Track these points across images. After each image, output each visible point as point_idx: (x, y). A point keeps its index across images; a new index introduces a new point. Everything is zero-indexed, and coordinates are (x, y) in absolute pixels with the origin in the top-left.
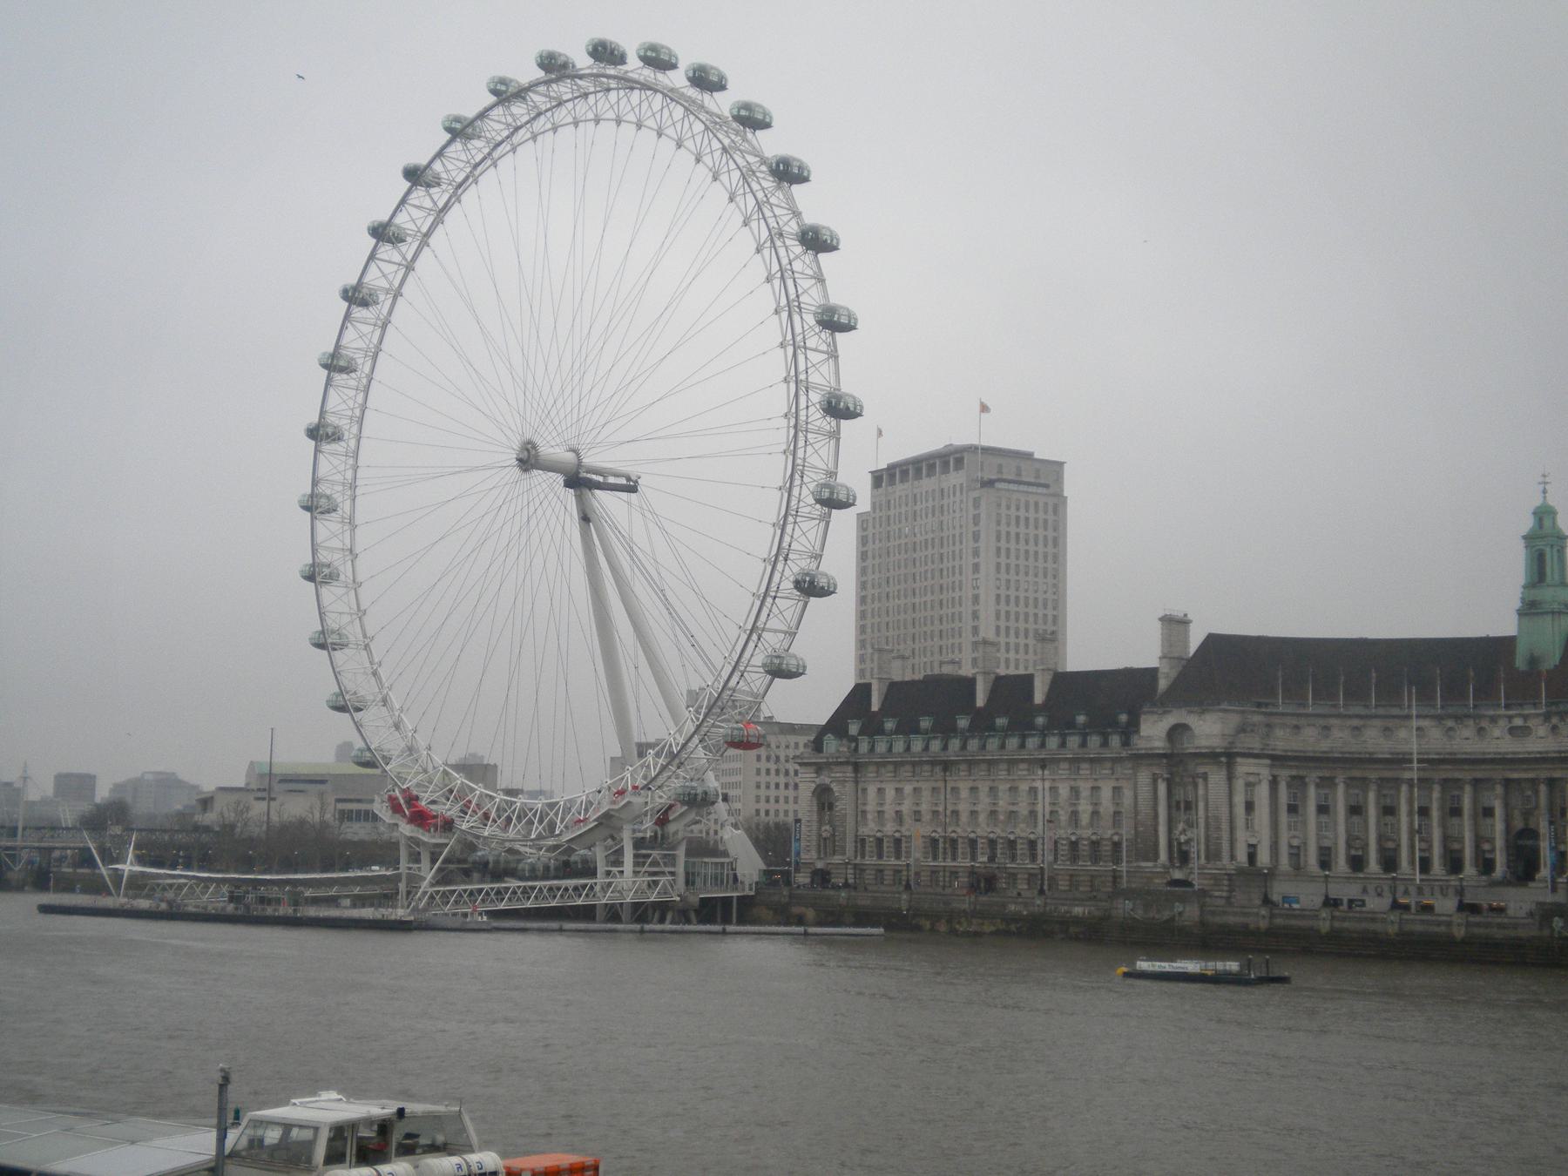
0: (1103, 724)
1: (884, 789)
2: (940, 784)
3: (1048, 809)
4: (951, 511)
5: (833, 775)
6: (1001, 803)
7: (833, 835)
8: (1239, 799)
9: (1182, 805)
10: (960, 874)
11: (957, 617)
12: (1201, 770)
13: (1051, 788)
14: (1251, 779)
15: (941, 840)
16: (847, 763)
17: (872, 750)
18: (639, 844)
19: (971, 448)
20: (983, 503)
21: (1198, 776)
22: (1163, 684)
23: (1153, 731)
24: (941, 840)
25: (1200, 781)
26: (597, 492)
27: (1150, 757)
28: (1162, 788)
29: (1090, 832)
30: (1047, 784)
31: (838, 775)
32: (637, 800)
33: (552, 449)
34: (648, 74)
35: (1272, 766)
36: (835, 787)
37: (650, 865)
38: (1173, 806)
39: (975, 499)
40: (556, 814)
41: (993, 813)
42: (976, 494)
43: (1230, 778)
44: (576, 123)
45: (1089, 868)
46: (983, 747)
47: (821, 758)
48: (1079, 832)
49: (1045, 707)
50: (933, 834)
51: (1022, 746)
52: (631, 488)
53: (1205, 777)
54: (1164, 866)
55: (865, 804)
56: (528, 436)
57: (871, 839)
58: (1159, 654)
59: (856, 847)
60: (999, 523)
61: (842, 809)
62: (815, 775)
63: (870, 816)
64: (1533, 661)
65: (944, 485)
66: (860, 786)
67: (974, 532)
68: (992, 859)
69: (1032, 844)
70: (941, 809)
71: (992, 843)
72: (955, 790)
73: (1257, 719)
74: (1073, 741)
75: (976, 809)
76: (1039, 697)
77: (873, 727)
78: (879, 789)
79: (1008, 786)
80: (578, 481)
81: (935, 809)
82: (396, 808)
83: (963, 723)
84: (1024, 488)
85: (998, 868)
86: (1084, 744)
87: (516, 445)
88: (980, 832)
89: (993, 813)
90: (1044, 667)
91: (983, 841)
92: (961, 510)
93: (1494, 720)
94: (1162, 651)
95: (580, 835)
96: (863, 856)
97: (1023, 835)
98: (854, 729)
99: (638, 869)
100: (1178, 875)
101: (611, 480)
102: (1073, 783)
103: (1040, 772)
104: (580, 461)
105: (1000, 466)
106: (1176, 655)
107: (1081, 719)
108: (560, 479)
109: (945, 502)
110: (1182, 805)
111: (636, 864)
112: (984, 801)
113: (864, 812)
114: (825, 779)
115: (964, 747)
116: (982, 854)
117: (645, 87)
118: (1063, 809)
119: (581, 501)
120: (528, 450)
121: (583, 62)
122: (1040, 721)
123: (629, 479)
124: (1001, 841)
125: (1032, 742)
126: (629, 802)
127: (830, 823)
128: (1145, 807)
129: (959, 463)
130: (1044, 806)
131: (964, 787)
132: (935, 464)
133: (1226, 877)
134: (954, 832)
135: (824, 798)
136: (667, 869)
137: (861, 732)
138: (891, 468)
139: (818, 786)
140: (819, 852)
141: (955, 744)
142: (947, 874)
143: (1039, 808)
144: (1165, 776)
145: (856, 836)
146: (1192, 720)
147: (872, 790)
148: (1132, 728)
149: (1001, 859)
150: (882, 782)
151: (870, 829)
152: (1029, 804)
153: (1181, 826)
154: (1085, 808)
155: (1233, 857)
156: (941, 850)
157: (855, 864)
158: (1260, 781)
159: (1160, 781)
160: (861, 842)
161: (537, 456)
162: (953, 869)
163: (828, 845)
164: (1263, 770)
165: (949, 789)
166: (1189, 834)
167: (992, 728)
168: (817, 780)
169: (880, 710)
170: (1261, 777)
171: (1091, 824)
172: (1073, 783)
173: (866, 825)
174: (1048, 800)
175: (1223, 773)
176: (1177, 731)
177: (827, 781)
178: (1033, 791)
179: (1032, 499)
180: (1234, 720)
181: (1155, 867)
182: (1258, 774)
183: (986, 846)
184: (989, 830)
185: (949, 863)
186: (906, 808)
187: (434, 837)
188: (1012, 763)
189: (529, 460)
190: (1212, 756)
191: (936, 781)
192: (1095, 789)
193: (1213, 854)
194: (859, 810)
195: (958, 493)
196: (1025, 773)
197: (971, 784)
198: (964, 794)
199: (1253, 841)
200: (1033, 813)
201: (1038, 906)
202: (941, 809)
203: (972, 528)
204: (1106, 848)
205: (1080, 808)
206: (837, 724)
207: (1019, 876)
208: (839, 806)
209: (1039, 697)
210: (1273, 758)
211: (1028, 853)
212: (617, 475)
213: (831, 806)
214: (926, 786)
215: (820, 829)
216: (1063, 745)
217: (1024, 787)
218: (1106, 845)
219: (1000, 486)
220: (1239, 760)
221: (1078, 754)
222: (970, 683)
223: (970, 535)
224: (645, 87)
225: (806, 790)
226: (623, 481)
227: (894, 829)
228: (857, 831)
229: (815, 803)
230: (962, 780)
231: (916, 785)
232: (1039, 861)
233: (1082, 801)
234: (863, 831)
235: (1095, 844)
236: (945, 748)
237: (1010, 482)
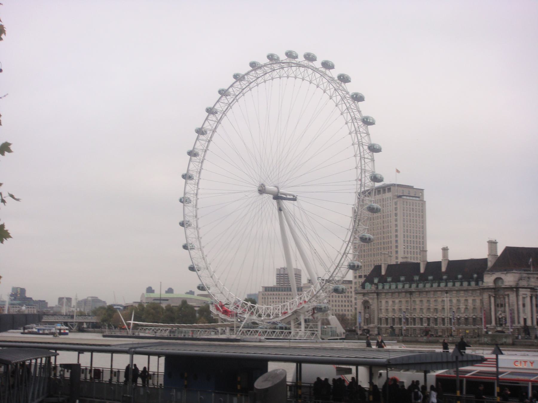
0: (468, 278)
1: (388, 301)
2: (409, 299)
4: (387, 206)
5: (369, 297)
6: (431, 305)
7: (370, 317)
8: (521, 303)
9: (499, 305)
10: (417, 330)
11: (390, 242)
12: (507, 293)
13: (450, 300)
14: (524, 296)
15: (410, 319)
16: (375, 293)
17: (383, 288)
18: (306, 321)
19: (393, 185)
20: (398, 203)
21: (505, 295)
22: (490, 264)
23: (489, 280)
24: (410, 319)
25: (506, 297)
26: (284, 201)
27: (488, 289)
28: (492, 299)
29: (464, 315)
30: (448, 299)
31: (371, 297)
32: (306, 306)
33: (270, 187)
34: (306, 63)
35: (530, 291)
36: (370, 301)
37: (310, 328)
38: (497, 306)
39: (395, 202)
40: (254, 310)
41: (429, 309)
42: (395, 200)
43: (517, 295)
44: (280, 77)
45: (464, 327)
46: (425, 286)
47: (365, 291)
48: (461, 315)
49: (446, 273)
51: (439, 286)
52: (294, 199)
53: (508, 295)
54: (494, 326)
55: (381, 307)
56: (262, 182)
57: (384, 318)
58: (488, 254)
59: (378, 321)
60: (404, 210)
62: (362, 297)
63: (383, 311)
65: (384, 197)
66: (379, 300)
67: (395, 213)
68: (428, 325)
69: (443, 319)
70: (409, 308)
71: (428, 319)
72: (414, 301)
73: (525, 275)
74: (458, 284)
75: (422, 307)
76: (444, 269)
77: (383, 280)
78: (386, 301)
80: (278, 197)
81: (407, 308)
82: (218, 309)
83: (416, 278)
84: (411, 198)
85: (431, 328)
86: (462, 285)
87: (258, 185)
88: (424, 315)
89: (429, 309)
90: (445, 259)
91: (425, 318)
92: (390, 206)
94: (489, 253)
95: (286, 318)
96: (381, 324)
97: (440, 316)
98: (376, 281)
99: (306, 329)
100: (499, 329)
101: (288, 197)
102: (458, 298)
103: (446, 295)
104: (279, 191)
105: (403, 191)
106: (494, 254)
107: (460, 276)
108: (272, 196)
109: (384, 203)
110: (499, 305)
111: (306, 328)
112: (425, 305)
113: (381, 309)
114: (366, 298)
115: (417, 286)
116: (425, 323)
117: (304, 66)
119: (279, 204)
120: (262, 187)
121: (301, 59)
122: (445, 277)
123: (294, 196)
124: (432, 318)
125: (443, 285)
126: (303, 307)
127: (368, 313)
128: (486, 305)
129: (389, 190)
130: (447, 305)
131: (418, 300)
132: (380, 190)
133: (517, 330)
134: (414, 316)
135: (366, 305)
136: (315, 329)
137: (379, 282)
139: (364, 301)
140: (364, 323)
141: (414, 286)
142: (412, 330)
143: (446, 307)
144: (494, 295)
145: (378, 317)
146: (503, 276)
147: (383, 302)
148: (480, 278)
149: (432, 325)
150: (387, 299)
151: (383, 315)
152: (442, 306)
153: (500, 312)
154: (462, 307)
155: (519, 323)
156: (410, 322)
157: (379, 327)
158: (527, 296)
159: (491, 297)
160: (380, 320)
161: (265, 189)
162: (414, 328)
163: (368, 321)
164: (528, 293)
165: (412, 301)
166: (503, 315)
167: (427, 280)
168: (364, 299)
169: (385, 274)
170: (527, 295)
171: (465, 312)
172: (458, 298)
173: (382, 314)
174: (449, 304)
175: (515, 294)
176: (497, 280)
177: (367, 299)
178: (443, 301)
179: (414, 201)
180: (517, 276)
181: (491, 326)
182: (526, 294)
183: (426, 320)
184: (427, 315)
185: (413, 326)
187: (231, 319)
188: (435, 291)
189: (262, 190)
190: (511, 288)
191: (407, 298)
192: (466, 300)
193: (513, 322)
194: (379, 308)
196: (463, 294)
197: (420, 299)
198: (418, 302)
199: (525, 317)
200: (443, 309)
201: (451, 340)
203: (394, 212)
204: (471, 320)
205: (461, 307)
206: (369, 279)
207: (439, 330)
208: (372, 307)
209: (444, 269)
210: (531, 288)
211: (441, 322)
212: (290, 195)
213: (368, 308)
214: (403, 300)
215: (365, 315)
216: (454, 285)
217: (440, 300)
218: (470, 319)
219: (404, 198)
220: (520, 289)
221: (460, 288)
222: (418, 264)
223: (394, 214)
224: (304, 66)
225: (359, 302)
226: (292, 197)
227: (392, 315)
228: (378, 316)
229: (363, 306)
230: (417, 298)
231: (400, 300)
232: (446, 325)
233: (461, 304)
234: (381, 316)
235: (466, 319)
236: (410, 287)
237: (407, 196)
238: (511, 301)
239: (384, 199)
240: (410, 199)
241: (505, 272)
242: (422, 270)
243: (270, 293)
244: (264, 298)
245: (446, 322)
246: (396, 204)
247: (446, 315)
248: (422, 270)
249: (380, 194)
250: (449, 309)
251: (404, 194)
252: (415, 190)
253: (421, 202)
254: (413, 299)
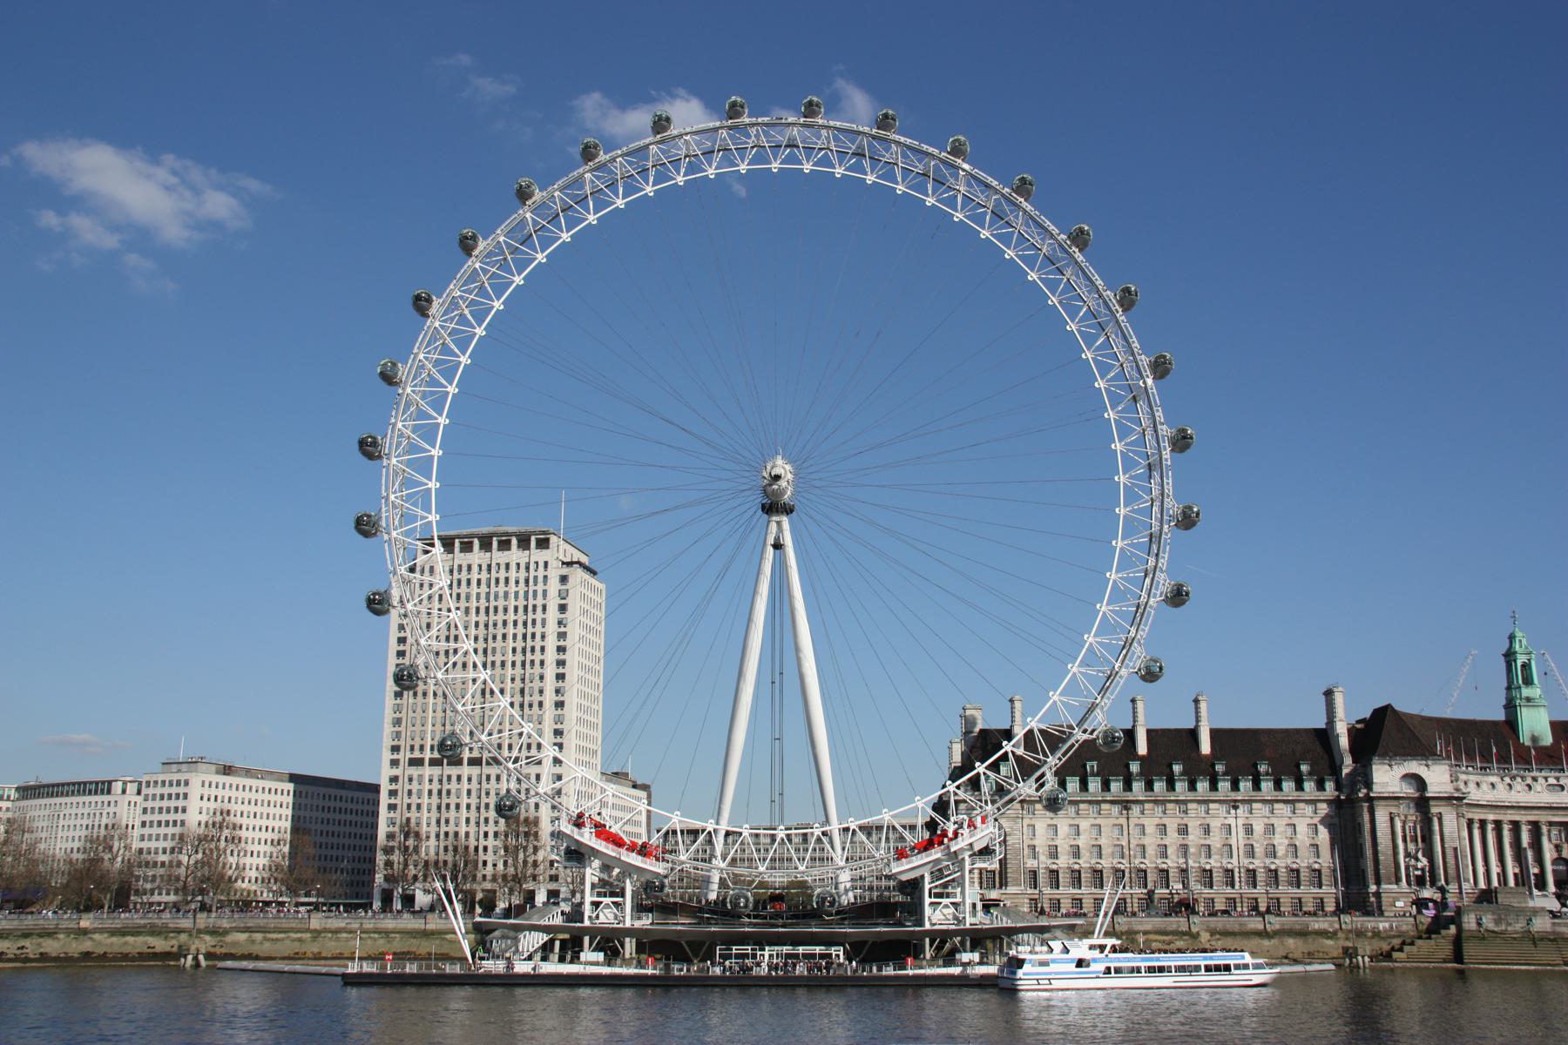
2: (1123, 821)
3: (1242, 843)
30: (1240, 822)
50: (1119, 866)
61: (1014, 844)
64: (1534, 739)
70: (1124, 844)
76: (1206, 748)
79: (1199, 823)
83: (1135, 767)
93: (1535, 779)
102: (1266, 821)
103: (1233, 811)
118: (1257, 842)
141: (1138, 786)
154: (1281, 842)
186: (1082, 841)
198: (1150, 829)
202: (1124, 843)
209: (1206, 748)
232: (1237, 887)
233: (1276, 836)
238: (1446, 830)
241: (1430, 762)
242: (1142, 748)
245: (1237, 879)
246: (564, 579)
247: (1235, 861)
248: (1142, 748)
250: (1241, 847)
254: (1133, 821)
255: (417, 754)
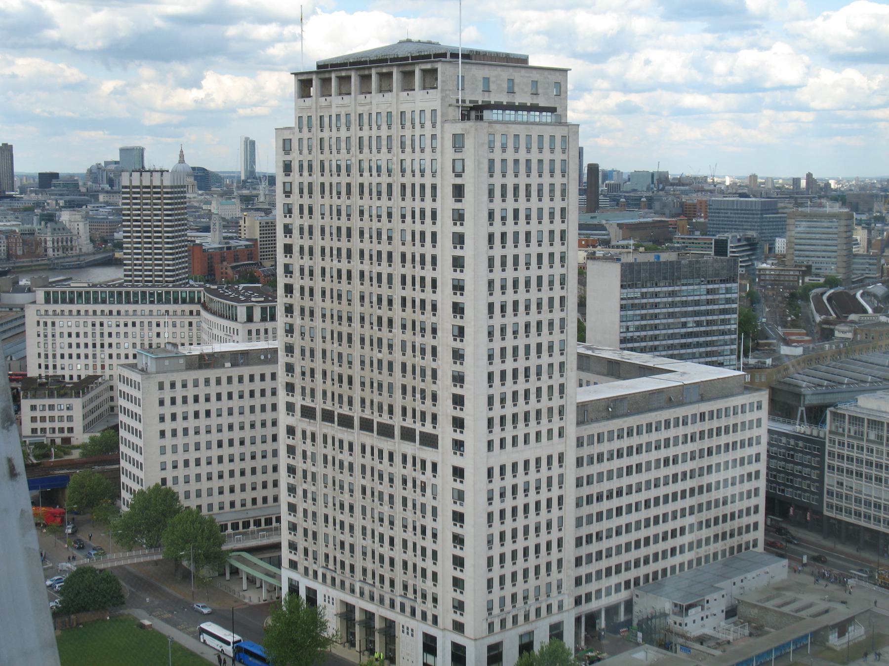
20: (469, 143)
65: (406, 107)
105: (487, 80)
138: (324, 68)
179: (535, 131)
195: (428, 124)
203: (453, 180)
219: (495, 117)
223: (449, 190)
239: (408, 116)
240: (515, 123)
243: (59, 307)
244: (42, 324)
246: (458, 142)
249: (391, 91)
251: (493, 99)
252: (535, 76)
253: (559, 132)
255: (308, 403)
